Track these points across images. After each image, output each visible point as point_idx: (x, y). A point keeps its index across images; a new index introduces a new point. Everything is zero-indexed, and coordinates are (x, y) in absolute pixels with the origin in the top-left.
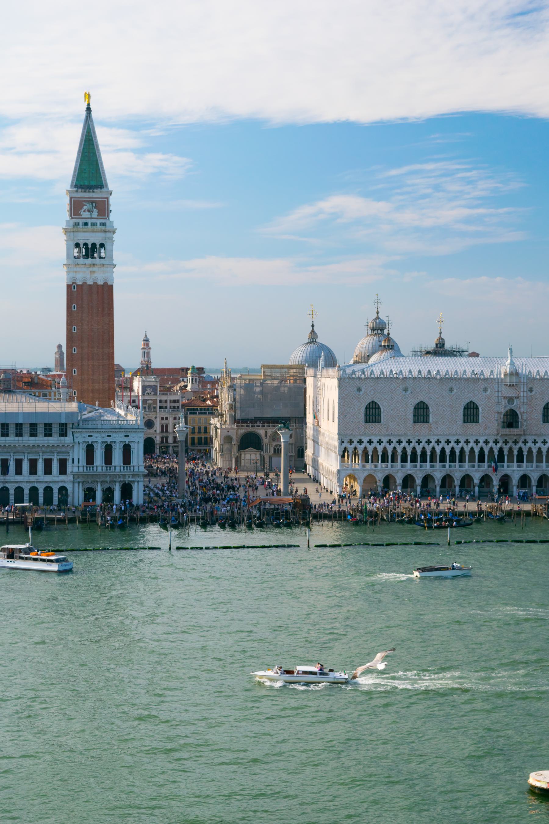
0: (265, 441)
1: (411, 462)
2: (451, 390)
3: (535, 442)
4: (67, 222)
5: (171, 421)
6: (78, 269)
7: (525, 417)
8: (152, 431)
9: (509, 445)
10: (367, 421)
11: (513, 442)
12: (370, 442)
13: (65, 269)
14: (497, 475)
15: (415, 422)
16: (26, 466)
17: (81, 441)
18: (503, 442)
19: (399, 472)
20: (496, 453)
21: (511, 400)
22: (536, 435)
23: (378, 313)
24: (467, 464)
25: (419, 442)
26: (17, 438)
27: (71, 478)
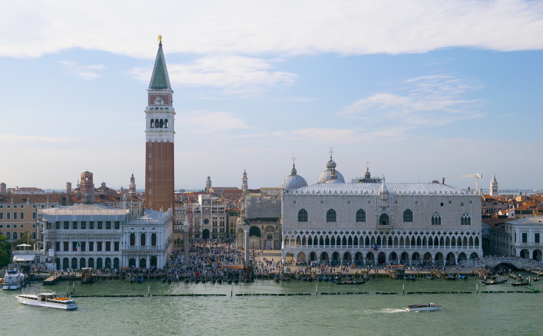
0: (262, 231)
1: (343, 244)
2: (349, 202)
3: (399, 233)
4: (147, 107)
5: (219, 220)
6: (152, 134)
7: (393, 218)
8: (208, 225)
9: (383, 235)
10: (299, 221)
12: (301, 233)
13: (145, 134)
15: (328, 221)
16: (95, 246)
17: (127, 232)
19: (319, 250)
20: (376, 240)
21: (384, 208)
22: (400, 229)
23: (331, 158)
24: (359, 246)
25: (330, 233)
26: (90, 230)
27: (121, 253)
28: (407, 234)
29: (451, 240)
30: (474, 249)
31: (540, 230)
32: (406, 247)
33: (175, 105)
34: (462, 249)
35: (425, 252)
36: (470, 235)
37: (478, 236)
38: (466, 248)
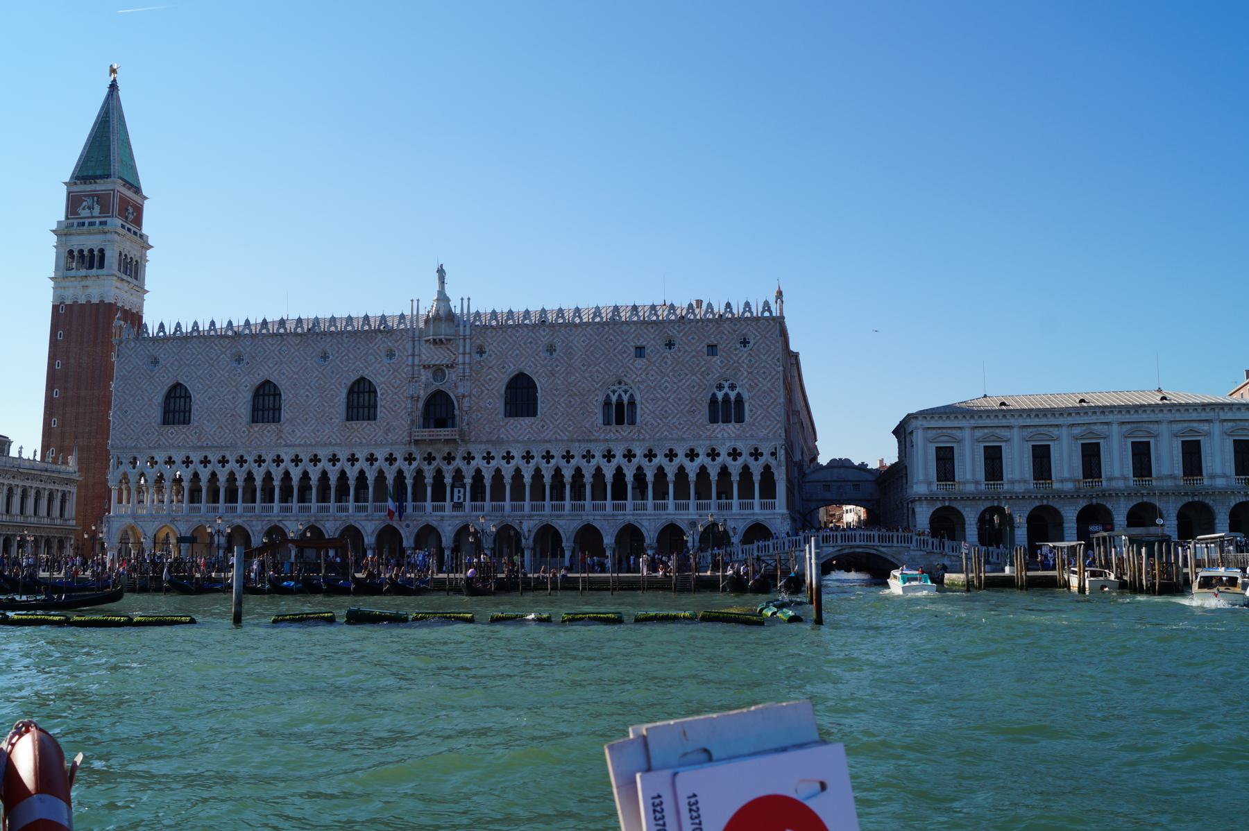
2: (325, 357)
3: (488, 458)
4: (59, 222)
6: (68, 284)
7: (466, 403)
9: (435, 464)
10: (166, 422)
11: (444, 458)
13: (52, 284)
14: (408, 526)
15: (254, 420)
18: (425, 459)
19: (220, 519)
21: (438, 371)
22: (488, 442)
25: (260, 461)
28: (518, 461)
29: (671, 477)
30: (757, 509)
31: (1004, 433)
32: (514, 508)
33: (150, 225)
34: (713, 511)
35: (576, 525)
36: (740, 461)
37: (772, 462)
38: (729, 507)
